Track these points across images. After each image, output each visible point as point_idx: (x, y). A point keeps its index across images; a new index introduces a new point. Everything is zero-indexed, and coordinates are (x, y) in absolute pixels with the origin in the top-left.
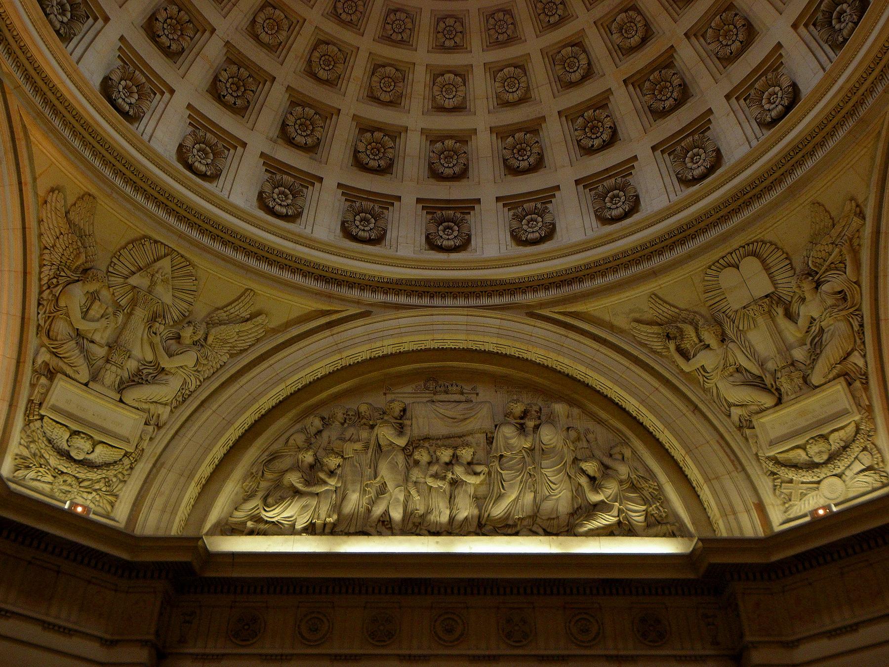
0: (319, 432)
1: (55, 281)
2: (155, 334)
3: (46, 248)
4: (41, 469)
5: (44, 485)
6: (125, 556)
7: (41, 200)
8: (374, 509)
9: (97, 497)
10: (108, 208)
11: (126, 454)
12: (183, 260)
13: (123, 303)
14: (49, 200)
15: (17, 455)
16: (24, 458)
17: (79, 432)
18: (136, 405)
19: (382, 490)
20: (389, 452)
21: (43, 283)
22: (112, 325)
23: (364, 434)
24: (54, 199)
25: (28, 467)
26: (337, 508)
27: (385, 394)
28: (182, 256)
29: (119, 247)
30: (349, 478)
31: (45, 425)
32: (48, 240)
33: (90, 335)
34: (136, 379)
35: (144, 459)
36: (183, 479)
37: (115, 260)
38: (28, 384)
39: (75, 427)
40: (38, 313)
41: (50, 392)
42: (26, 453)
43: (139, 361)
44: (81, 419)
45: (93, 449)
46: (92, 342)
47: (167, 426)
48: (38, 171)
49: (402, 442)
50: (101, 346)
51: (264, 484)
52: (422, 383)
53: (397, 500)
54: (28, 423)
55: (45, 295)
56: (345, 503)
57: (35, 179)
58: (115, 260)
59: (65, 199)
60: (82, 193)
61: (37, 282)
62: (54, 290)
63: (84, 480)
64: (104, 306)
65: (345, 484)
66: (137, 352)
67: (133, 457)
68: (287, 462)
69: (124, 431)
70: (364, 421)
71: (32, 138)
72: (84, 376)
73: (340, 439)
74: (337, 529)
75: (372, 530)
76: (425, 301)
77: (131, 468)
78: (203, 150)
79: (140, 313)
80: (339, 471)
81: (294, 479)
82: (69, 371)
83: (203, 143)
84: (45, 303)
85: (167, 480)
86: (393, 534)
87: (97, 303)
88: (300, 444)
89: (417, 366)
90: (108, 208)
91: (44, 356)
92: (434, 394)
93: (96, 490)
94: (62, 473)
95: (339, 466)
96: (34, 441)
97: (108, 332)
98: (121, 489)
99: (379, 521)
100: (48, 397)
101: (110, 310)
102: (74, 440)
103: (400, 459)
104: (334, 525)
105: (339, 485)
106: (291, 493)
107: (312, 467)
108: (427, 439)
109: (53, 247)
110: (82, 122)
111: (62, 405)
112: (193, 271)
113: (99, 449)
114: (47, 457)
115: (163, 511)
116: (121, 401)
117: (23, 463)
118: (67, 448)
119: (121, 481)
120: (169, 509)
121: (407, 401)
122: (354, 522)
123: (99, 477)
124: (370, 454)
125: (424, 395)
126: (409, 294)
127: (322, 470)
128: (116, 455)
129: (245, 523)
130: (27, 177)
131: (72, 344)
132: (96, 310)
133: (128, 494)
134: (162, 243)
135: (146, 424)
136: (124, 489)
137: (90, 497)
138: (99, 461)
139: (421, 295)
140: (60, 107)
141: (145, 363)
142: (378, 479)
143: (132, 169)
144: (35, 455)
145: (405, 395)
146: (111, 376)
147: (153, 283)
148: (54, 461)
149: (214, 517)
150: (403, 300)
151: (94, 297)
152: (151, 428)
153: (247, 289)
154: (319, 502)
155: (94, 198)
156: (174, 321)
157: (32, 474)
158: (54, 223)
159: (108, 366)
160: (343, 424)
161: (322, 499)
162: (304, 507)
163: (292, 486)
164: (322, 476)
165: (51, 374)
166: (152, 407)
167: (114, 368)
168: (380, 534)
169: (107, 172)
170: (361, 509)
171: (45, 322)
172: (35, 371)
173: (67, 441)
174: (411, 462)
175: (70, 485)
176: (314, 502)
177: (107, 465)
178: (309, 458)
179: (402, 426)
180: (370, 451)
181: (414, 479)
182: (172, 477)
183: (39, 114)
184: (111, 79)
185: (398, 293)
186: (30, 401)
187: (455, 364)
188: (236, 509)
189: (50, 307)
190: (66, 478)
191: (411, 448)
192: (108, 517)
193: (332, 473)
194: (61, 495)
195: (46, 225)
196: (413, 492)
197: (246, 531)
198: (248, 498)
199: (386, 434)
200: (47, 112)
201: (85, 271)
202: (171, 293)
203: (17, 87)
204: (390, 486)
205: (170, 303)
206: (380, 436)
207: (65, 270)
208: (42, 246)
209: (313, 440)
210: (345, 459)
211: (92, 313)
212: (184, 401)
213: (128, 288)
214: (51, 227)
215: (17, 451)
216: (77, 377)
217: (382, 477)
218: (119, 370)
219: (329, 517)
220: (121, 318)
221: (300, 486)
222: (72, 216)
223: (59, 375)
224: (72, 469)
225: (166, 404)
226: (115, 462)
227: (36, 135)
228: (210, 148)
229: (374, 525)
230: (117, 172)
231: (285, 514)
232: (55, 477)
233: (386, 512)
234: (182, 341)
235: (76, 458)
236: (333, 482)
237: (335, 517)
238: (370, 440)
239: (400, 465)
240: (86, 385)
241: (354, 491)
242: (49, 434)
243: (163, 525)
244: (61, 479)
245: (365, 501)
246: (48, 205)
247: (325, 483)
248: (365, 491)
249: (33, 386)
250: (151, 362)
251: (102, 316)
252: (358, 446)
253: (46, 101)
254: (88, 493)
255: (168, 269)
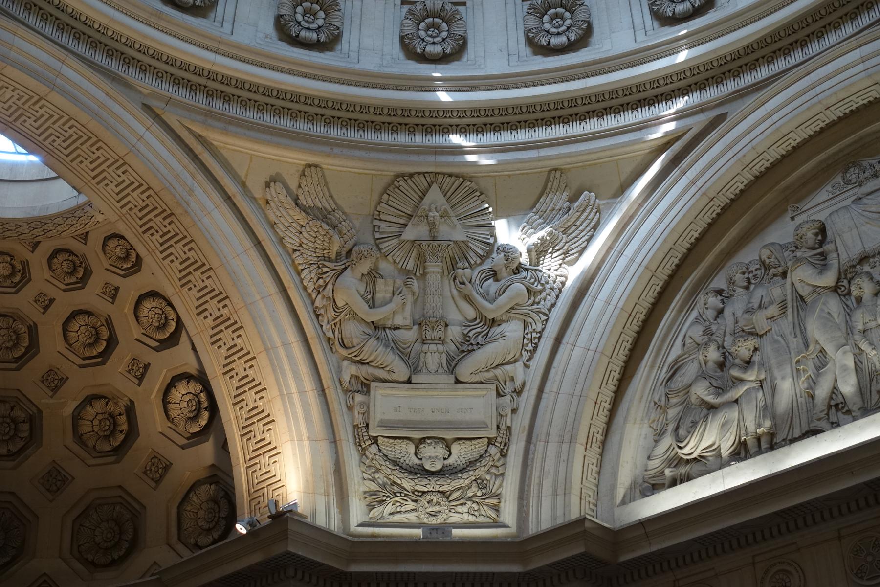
0: (720, 312)
1: (321, 281)
2: (464, 283)
3: (294, 251)
4: (396, 499)
5: (407, 515)
6: (516, 568)
7: (262, 203)
8: (817, 393)
9: (475, 506)
10: (339, 168)
11: (491, 442)
12: (453, 179)
13: (410, 266)
14: (269, 197)
15: (365, 492)
16: (373, 493)
17: (424, 439)
18: (476, 378)
19: (822, 360)
20: (815, 301)
21: (309, 291)
22: (410, 299)
23: (777, 292)
24: (274, 194)
25: (382, 502)
26: (767, 410)
27: (793, 218)
28: (450, 175)
29: (373, 204)
30: (773, 361)
31: (382, 447)
32: (292, 241)
33: (390, 322)
34: (465, 348)
35: (514, 438)
36: (565, 447)
37: (376, 223)
38: (345, 409)
39: (417, 435)
40: (322, 326)
41: (372, 409)
42: (374, 487)
43: (460, 325)
44: (421, 422)
45: (450, 451)
46: (397, 328)
47: (527, 388)
48: (242, 174)
49: (829, 279)
50: (408, 328)
51: (672, 413)
52: (839, 178)
53: (845, 368)
54: (363, 452)
55: (319, 302)
56: (777, 397)
57: (243, 185)
58: (376, 223)
59: (286, 187)
60: (301, 168)
61: (304, 294)
62: (325, 293)
63: (452, 492)
64: (390, 282)
65: (769, 371)
66: (453, 315)
67: (500, 440)
68: (690, 370)
69: (477, 415)
70: (772, 271)
71: (215, 143)
72: (401, 371)
73: (747, 311)
74: (778, 439)
75: (823, 424)
76: (798, 56)
77: (504, 455)
78: (433, 26)
79: (434, 268)
80: (756, 358)
81: (702, 391)
82: (382, 374)
83: (428, 17)
84: (322, 311)
85: (547, 454)
86: (855, 419)
87: (380, 281)
88: (699, 340)
89: (822, 156)
90: (339, 168)
91: (349, 370)
92: (860, 186)
93: (470, 499)
94: (423, 492)
95: (756, 349)
96: (378, 471)
97: (408, 308)
98: (501, 486)
99: (830, 407)
100: (371, 414)
101: (399, 282)
102: (422, 450)
103: (833, 305)
104: (772, 435)
105: (762, 377)
106: (705, 411)
107: (721, 365)
108: (864, 259)
109: (301, 245)
110: (261, 90)
111: (391, 416)
112: (473, 185)
113: (455, 448)
114: (399, 482)
115: (555, 494)
116: (458, 382)
117: (374, 499)
118: (417, 461)
119: (497, 476)
120: (560, 491)
121: (822, 216)
122: (796, 420)
123: (467, 482)
124: (790, 318)
125: (847, 194)
126: (770, 59)
127: (734, 365)
128: (479, 447)
129: (662, 473)
130: (231, 188)
131: (373, 342)
132: (383, 290)
133: (509, 489)
134: (419, 173)
135: (499, 395)
136: (504, 484)
137: (465, 509)
138: (461, 462)
139: (786, 51)
140: (230, 90)
141: (469, 323)
142: (811, 347)
143: (344, 107)
144: (384, 486)
145: (820, 206)
146: (433, 358)
147: (432, 227)
148: (407, 484)
149: (625, 477)
150: (764, 72)
151: (373, 276)
152: (508, 398)
153: (550, 171)
154: (741, 412)
155: (316, 166)
156: (480, 257)
157: (389, 508)
158: (289, 218)
159: (426, 347)
160: (747, 288)
161: (744, 406)
162: (723, 425)
163: (704, 403)
164: (735, 372)
165: (365, 386)
166: (498, 372)
167: (433, 347)
168: (835, 425)
169: (318, 129)
170: (800, 400)
171: (334, 333)
172: (346, 391)
173: (416, 454)
174: (852, 302)
175: (438, 504)
176: (733, 414)
177: (471, 464)
178: (713, 354)
179: (824, 256)
180: (789, 311)
181: (860, 327)
182: (552, 448)
183: (209, 114)
184: (281, 16)
185: (753, 66)
186: (356, 427)
187: (868, 129)
188: (649, 458)
189: (331, 314)
190: (429, 497)
191: (845, 283)
192: (495, 524)
193: (748, 364)
194: (431, 518)
195: (280, 226)
196: (864, 346)
197: (667, 483)
198: (659, 435)
199: (804, 277)
200: (217, 106)
201: (349, 252)
202: (459, 226)
203: (168, 101)
204: (829, 349)
205: (465, 239)
206: (798, 286)
207: (326, 263)
208: (291, 251)
209: (714, 328)
210: (761, 336)
211: (379, 296)
212: (535, 348)
213: (408, 245)
214: (288, 225)
215: (363, 489)
216: (394, 377)
217: (817, 342)
218: (440, 347)
219: (759, 426)
220: (415, 285)
221: (710, 399)
222: (302, 201)
223: (373, 385)
224: (433, 484)
225: (516, 361)
226: (481, 456)
227: (216, 138)
228: (439, 17)
229: (823, 415)
230: (328, 122)
231: (705, 444)
232: (416, 501)
233: (835, 390)
234: (499, 276)
235: (433, 469)
236: (751, 376)
237: (768, 423)
238: (785, 295)
239: (835, 316)
240: (409, 381)
241: (783, 378)
242: (391, 455)
243: (560, 512)
244: (423, 501)
245: (802, 385)
246: (271, 203)
247: (742, 381)
248: (798, 370)
249: (350, 408)
250: (475, 319)
251: (393, 294)
252: (773, 310)
253: (210, 94)
254: (462, 504)
255: (441, 201)
